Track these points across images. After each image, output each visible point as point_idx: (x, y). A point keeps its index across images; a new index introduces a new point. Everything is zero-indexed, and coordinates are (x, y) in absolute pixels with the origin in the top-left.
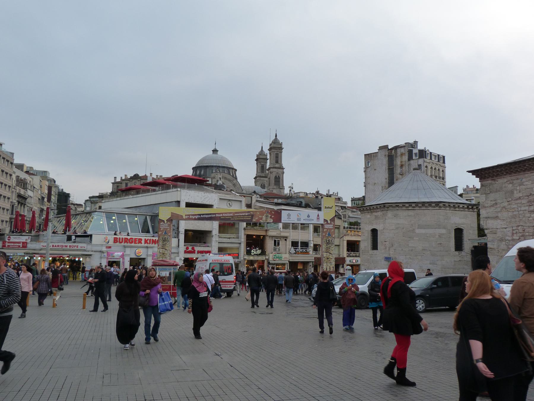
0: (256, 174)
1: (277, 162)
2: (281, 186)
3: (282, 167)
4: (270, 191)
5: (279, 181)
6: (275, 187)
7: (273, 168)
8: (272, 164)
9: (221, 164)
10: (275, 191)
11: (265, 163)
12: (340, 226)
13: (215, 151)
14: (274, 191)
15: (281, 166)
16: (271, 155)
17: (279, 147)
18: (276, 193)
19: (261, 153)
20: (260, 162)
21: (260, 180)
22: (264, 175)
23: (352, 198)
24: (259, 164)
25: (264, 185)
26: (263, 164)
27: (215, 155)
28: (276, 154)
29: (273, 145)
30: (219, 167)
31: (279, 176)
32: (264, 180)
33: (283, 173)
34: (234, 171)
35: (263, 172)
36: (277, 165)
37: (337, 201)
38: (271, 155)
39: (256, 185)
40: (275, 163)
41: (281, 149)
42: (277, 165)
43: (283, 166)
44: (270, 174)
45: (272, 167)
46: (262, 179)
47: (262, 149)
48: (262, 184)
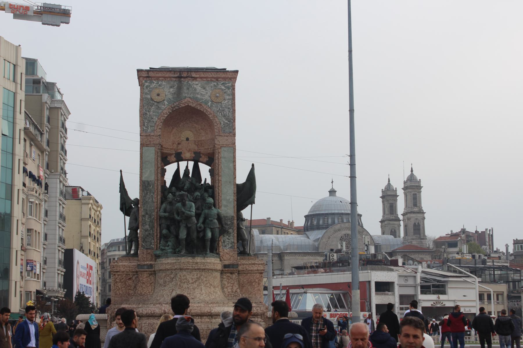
0: (383, 216)
1: (415, 205)
2: (422, 235)
3: (422, 211)
4: (409, 243)
5: (419, 230)
6: (414, 237)
7: (411, 212)
8: (409, 208)
9: (344, 210)
10: (415, 243)
11: (395, 201)
12: (503, 292)
13: (332, 192)
14: (413, 243)
15: (420, 210)
16: (406, 196)
17: (417, 186)
18: (416, 245)
19: (388, 189)
20: (388, 201)
21: (389, 224)
22: (393, 218)
23: (514, 240)
24: (386, 203)
25: (395, 230)
26: (392, 202)
27: (331, 197)
28: (413, 194)
29: (409, 184)
30: (342, 214)
31: (418, 223)
32: (394, 224)
33: (424, 218)
34: (359, 217)
35: (393, 214)
36: (416, 209)
37: (498, 261)
38: (406, 196)
39: (383, 233)
40: (413, 207)
41: (419, 187)
42: (416, 209)
43: (423, 210)
44: (406, 220)
45: (409, 211)
46: (391, 222)
47: (389, 184)
48: (392, 230)
